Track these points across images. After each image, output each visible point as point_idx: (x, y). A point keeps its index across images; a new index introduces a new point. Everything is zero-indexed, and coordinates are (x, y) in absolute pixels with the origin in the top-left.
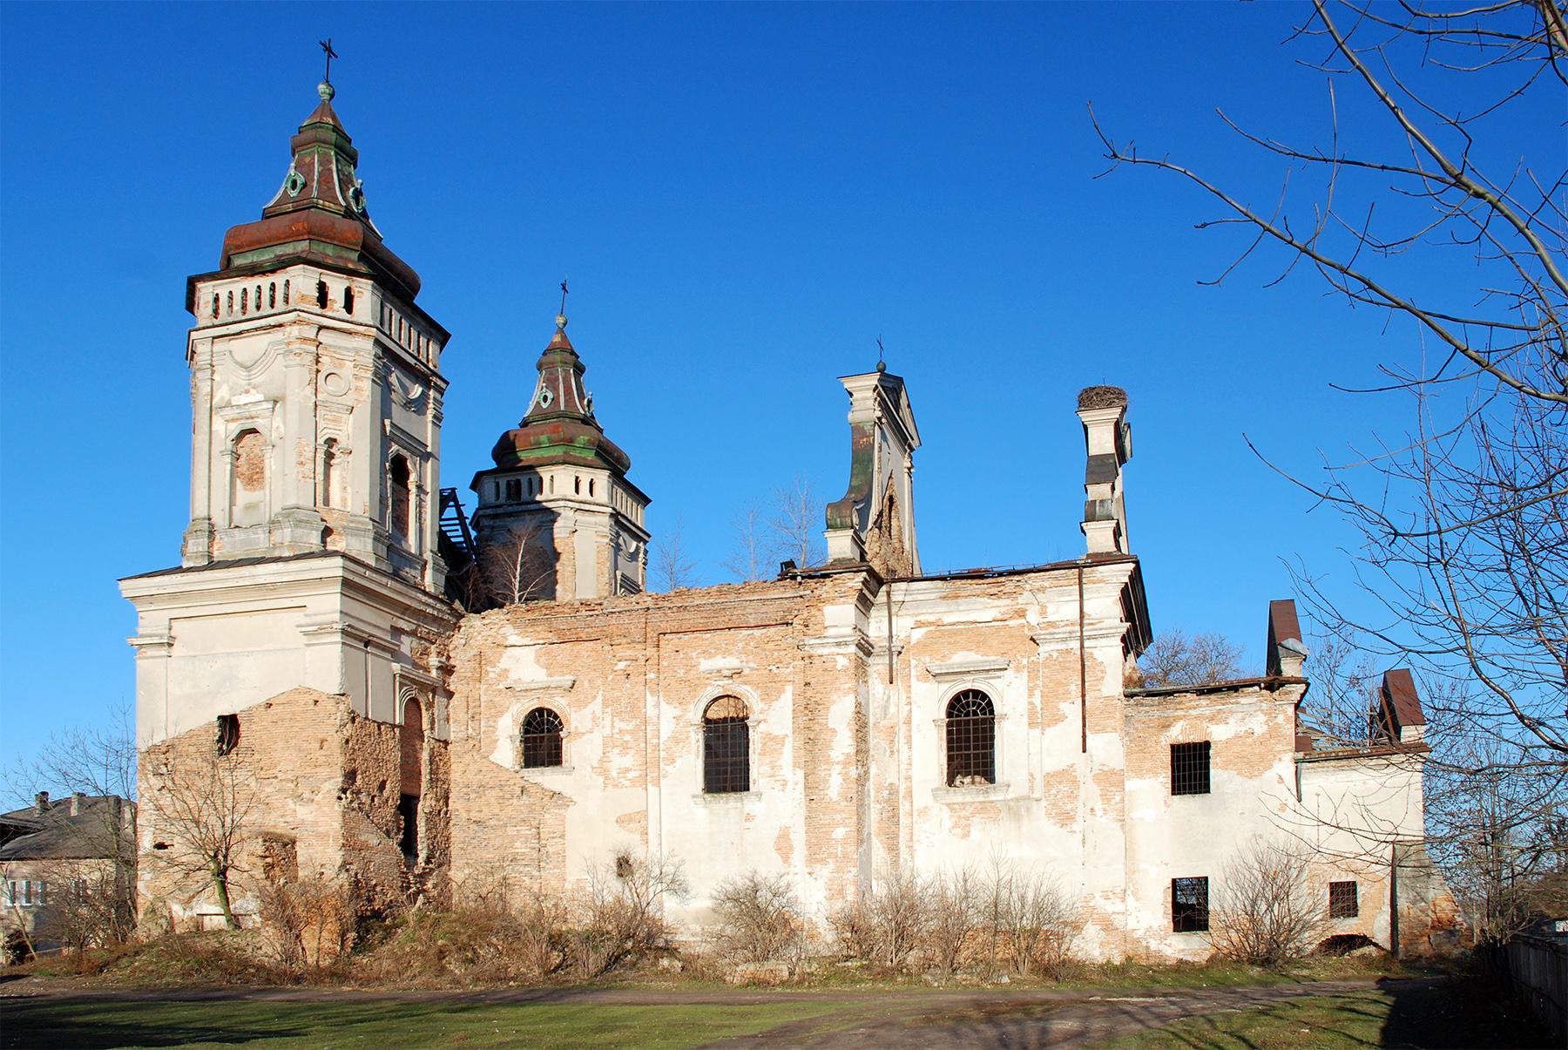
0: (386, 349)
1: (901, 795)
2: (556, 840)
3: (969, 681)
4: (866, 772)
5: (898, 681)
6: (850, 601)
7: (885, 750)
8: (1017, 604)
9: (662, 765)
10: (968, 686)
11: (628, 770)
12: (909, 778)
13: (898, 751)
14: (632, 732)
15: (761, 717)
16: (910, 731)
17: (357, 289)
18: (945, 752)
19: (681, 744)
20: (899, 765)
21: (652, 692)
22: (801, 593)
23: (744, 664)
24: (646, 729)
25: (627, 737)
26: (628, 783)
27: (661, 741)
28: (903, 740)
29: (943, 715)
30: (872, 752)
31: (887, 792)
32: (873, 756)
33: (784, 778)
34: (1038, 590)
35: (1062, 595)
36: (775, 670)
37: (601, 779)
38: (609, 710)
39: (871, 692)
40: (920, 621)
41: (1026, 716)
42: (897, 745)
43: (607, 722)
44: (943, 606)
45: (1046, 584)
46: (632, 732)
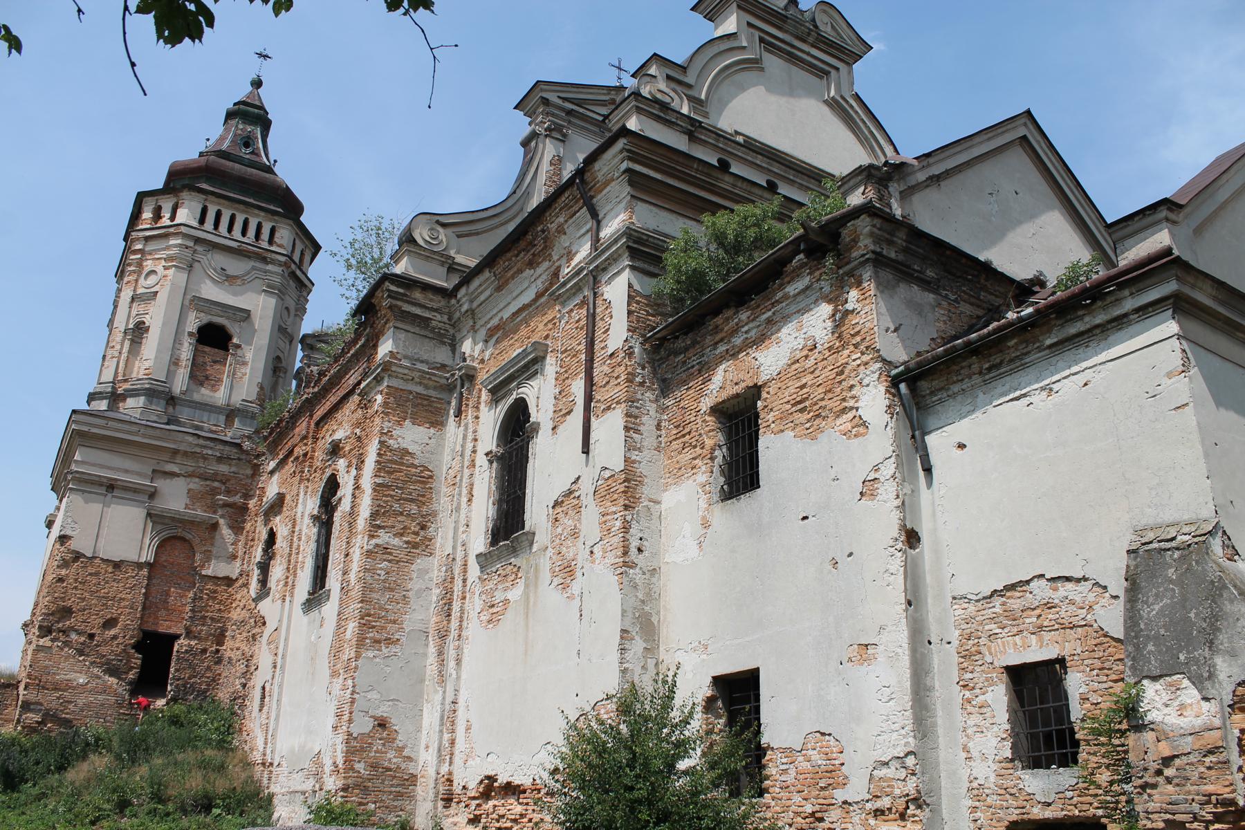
0: (198, 240)
45: (561, 219)
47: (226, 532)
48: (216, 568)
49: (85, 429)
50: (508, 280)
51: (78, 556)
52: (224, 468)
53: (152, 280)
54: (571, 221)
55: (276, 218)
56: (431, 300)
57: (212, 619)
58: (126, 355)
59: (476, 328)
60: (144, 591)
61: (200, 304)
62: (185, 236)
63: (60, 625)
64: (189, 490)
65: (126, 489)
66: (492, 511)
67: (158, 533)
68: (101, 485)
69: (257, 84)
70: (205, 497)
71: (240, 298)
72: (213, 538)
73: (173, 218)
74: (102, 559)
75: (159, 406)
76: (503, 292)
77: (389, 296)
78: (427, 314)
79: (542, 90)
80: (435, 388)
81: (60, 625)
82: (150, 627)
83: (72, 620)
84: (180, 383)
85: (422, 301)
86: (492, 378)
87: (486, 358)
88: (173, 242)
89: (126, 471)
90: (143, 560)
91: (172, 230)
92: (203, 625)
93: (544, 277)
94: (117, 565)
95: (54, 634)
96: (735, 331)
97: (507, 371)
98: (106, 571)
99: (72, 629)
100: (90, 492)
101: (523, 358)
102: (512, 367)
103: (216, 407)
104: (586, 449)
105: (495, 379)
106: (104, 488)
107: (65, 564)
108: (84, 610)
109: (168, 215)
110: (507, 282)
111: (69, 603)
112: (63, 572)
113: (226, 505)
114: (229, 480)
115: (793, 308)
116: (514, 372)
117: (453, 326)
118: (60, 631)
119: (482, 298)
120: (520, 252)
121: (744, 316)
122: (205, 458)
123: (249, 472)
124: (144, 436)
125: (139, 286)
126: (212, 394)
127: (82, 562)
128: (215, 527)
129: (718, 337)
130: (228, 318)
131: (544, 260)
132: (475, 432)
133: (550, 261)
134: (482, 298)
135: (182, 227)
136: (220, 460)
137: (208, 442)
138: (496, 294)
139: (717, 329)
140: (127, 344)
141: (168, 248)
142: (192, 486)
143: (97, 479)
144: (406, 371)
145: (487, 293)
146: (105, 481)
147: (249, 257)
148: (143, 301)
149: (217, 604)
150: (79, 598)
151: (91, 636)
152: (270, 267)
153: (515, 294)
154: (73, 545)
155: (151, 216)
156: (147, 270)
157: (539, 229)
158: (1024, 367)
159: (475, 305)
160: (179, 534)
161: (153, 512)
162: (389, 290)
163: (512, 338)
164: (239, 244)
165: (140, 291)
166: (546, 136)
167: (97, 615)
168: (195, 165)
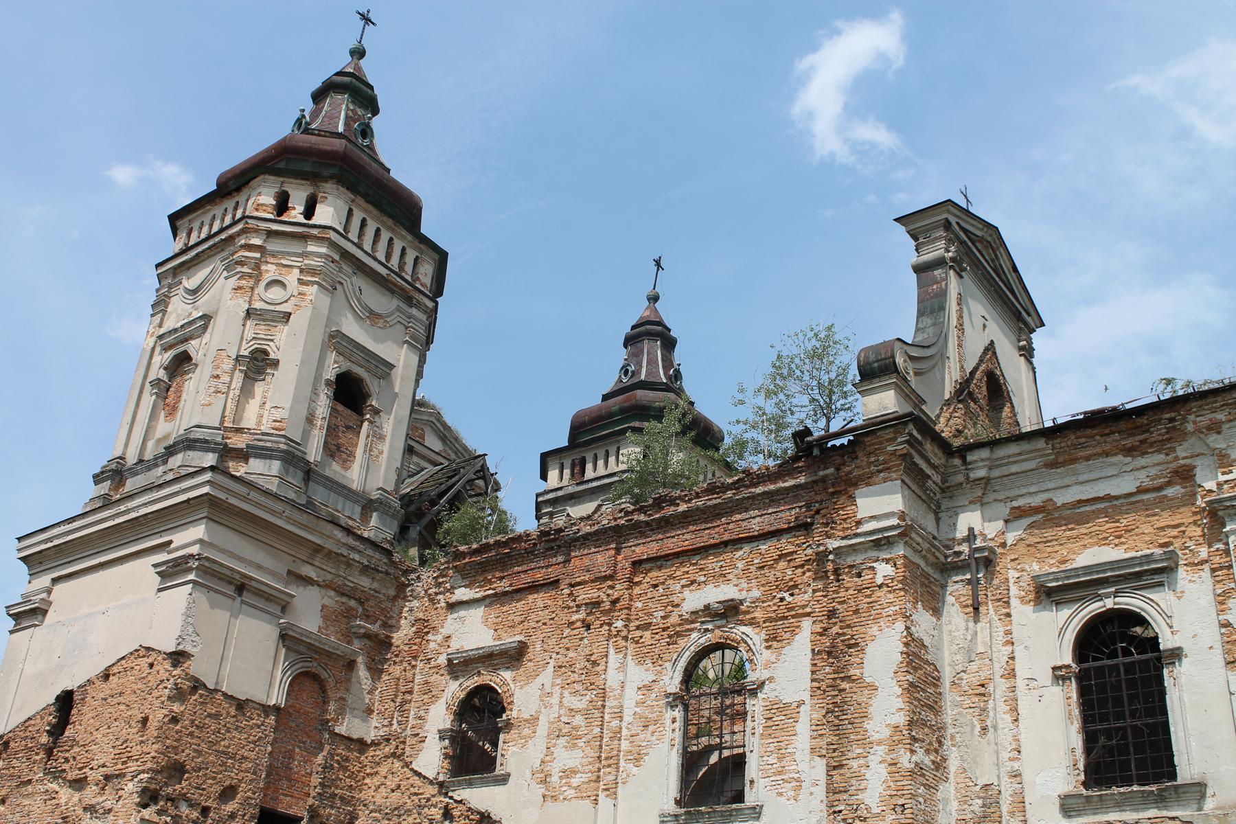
0: (345, 255)
1: (1005, 809)
3: (1108, 596)
4: (939, 766)
5: (990, 611)
6: (894, 475)
7: (973, 726)
8: (1177, 458)
9: (622, 763)
10: (1109, 603)
11: (574, 772)
12: (1016, 775)
13: (995, 727)
14: (586, 713)
15: (765, 675)
16: (1013, 689)
17: (322, 194)
18: (1076, 725)
19: (651, 728)
20: (997, 752)
21: (618, 650)
22: (821, 473)
23: (744, 593)
24: (604, 706)
26: (571, 793)
27: (624, 724)
28: (1002, 707)
29: (1067, 658)
30: (950, 730)
31: (980, 802)
32: (952, 737)
33: (796, 776)
34: (1209, 428)
36: (789, 599)
38: (559, 681)
39: (945, 628)
40: (1019, 507)
41: (1218, 650)
42: (991, 714)
43: (555, 700)
44: (1053, 479)
45: (1221, 416)
46: (586, 713)
47: (362, 673)
48: (348, 726)
49: (222, 496)
51: (197, 685)
52: (365, 582)
53: (275, 294)
55: (422, 246)
56: (935, 455)
57: (342, 799)
58: (237, 392)
59: (985, 500)
60: (269, 748)
61: (338, 341)
62: (333, 245)
63: (170, 790)
64: (323, 606)
65: (259, 593)
66: (1077, 741)
67: (292, 665)
68: (230, 583)
69: (358, 53)
70: (337, 618)
71: (382, 346)
72: (349, 680)
73: (309, 212)
74: (225, 694)
75: (296, 479)
76: (1058, 470)
77: (907, 442)
78: (929, 471)
79: (949, 212)
80: (932, 565)
81: (170, 790)
82: (270, 805)
83: (184, 783)
84: (314, 452)
85: (930, 455)
86: (1062, 575)
87: (1009, 542)
88: (312, 248)
89: (259, 567)
90: (272, 702)
91: (315, 232)
92: (332, 807)
93: (1154, 471)
94: (241, 705)
95: (162, 803)
97: (1098, 572)
98: (228, 713)
99: (184, 798)
100: (217, 591)
101: (1141, 564)
102: (1112, 570)
103: (350, 490)
105: (1068, 578)
106: (233, 588)
107: (179, 695)
108: (200, 769)
109: (301, 209)
110: (1074, 461)
111: (182, 757)
112: (177, 707)
113: (368, 636)
114: (368, 600)
116: (1112, 576)
117: (943, 490)
118: (170, 799)
119: (1014, 469)
120: (1113, 433)
122: (349, 564)
123: (392, 592)
124: (289, 520)
125: (256, 297)
126: (342, 472)
127: (201, 696)
128: (351, 665)
130: (368, 370)
131: (1159, 451)
132: (1008, 633)
133: (1167, 455)
134: (1014, 469)
135: (331, 232)
136: (366, 570)
137: (358, 543)
138: (1044, 470)
140: (238, 379)
141: (305, 255)
142: (327, 601)
143: (228, 573)
144: (919, 540)
146: (237, 577)
147: (393, 292)
148: (264, 320)
149: (349, 777)
150: (195, 751)
151: (205, 811)
152: (414, 311)
154: (196, 667)
155: (274, 203)
156: (267, 277)
157: (1167, 416)
159: (996, 473)
160: (314, 670)
161: (291, 633)
162: (910, 435)
163: (1073, 529)
164: (389, 272)
165: (258, 305)
166: (951, 267)
167: (214, 778)
168: (329, 148)
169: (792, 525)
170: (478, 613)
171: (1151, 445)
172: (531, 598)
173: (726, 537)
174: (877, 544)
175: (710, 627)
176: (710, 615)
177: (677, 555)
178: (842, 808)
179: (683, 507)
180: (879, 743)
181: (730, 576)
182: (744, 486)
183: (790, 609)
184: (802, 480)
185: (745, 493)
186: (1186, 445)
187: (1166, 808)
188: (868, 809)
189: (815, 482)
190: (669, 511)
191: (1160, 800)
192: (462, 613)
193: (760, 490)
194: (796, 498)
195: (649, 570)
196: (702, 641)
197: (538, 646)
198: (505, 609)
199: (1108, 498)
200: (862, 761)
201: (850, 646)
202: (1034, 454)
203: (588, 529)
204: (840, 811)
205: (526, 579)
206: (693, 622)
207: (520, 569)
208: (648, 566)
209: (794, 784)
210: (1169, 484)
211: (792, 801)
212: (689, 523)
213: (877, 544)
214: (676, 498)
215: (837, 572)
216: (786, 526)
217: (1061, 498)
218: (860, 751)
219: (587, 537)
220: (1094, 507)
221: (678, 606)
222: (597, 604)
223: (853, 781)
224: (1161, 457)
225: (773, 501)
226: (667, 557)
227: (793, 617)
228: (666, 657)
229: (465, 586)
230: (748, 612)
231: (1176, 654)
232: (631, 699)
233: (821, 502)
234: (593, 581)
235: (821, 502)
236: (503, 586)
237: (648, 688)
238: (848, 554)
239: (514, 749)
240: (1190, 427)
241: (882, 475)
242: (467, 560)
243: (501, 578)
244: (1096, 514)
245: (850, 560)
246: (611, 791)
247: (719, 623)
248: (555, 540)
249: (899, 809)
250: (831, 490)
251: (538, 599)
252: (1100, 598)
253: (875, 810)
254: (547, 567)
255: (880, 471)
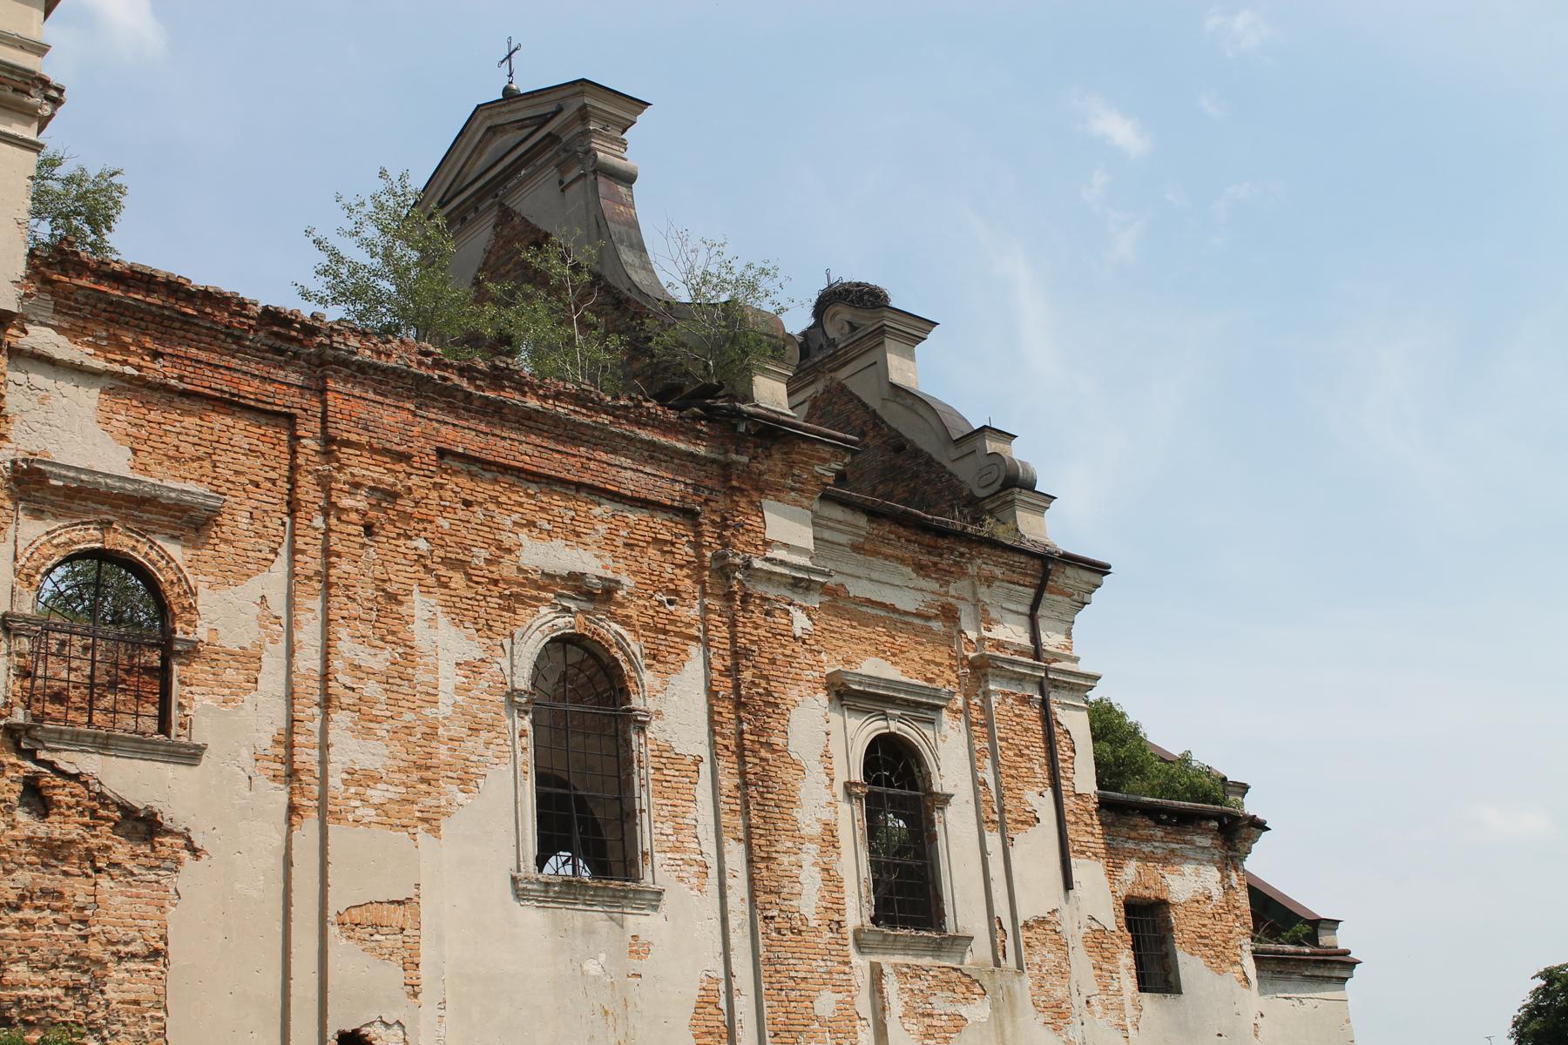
2: (131, 965)
19: (484, 735)
25: (372, 689)
34: (987, 579)
35: (1009, 598)
37: (282, 797)
45: (998, 572)
50: (879, 553)
54: (1006, 585)
76: (859, 557)
86: (868, 681)
93: (929, 597)
96: (1149, 839)
97: (894, 690)
101: (928, 696)
102: (906, 692)
104: (1068, 884)
105: (870, 685)
110: (875, 553)
115: (1191, 854)
116: (901, 699)
121: (1159, 833)
129: (1133, 834)
133: (941, 586)
138: (848, 550)
139: (1134, 827)
145: (843, 539)
153: (874, 575)
157: (962, 550)
158: (1289, 980)
163: (854, 627)
169: (676, 504)
170: (88, 398)
171: (938, 570)
172: (219, 421)
173: (587, 479)
174: (796, 584)
175: (573, 606)
176: (577, 589)
177: (505, 469)
178: (775, 913)
179: (533, 403)
180: (811, 840)
181: (587, 539)
182: (626, 418)
183: (673, 622)
184: (701, 450)
185: (626, 428)
186: (959, 584)
187: (938, 957)
188: (804, 920)
189: (713, 461)
190: (511, 396)
191: (937, 948)
192: (39, 379)
193: (644, 434)
194: (681, 469)
195: (456, 473)
196: (560, 622)
197: (243, 521)
198: (153, 416)
199: (892, 609)
200: (793, 858)
201: (767, 703)
202: (850, 529)
203: (366, 355)
204: (772, 918)
205: (220, 383)
206: (540, 588)
207: (203, 356)
208: (457, 465)
209: (696, 868)
210: (936, 617)
211: (695, 892)
212: (531, 430)
213: (796, 584)
214: (527, 384)
215: (745, 599)
216: (669, 503)
217: (858, 589)
218: (790, 844)
219: (363, 368)
220: (874, 612)
221: (509, 551)
222: (393, 496)
223: (785, 882)
224: (935, 586)
225: (652, 457)
226: (486, 464)
227: (677, 634)
228: (498, 626)
229: (59, 330)
230: (621, 605)
231: (946, 799)
232: (448, 679)
233: (712, 490)
234: (373, 450)
235: (712, 490)
236: (158, 370)
237: (472, 668)
238: (760, 580)
239: (208, 701)
240: (972, 570)
241: (793, 494)
242: (84, 282)
243: (156, 355)
244: (877, 620)
245: (760, 589)
246: (430, 821)
247: (589, 606)
248: (293, 339)
249: (834, 926)
250: (735, 483)
251: (240, 432)
252: (886, 717)
253: (813, 923)
254: (264, 379)
255: (793, 489)
